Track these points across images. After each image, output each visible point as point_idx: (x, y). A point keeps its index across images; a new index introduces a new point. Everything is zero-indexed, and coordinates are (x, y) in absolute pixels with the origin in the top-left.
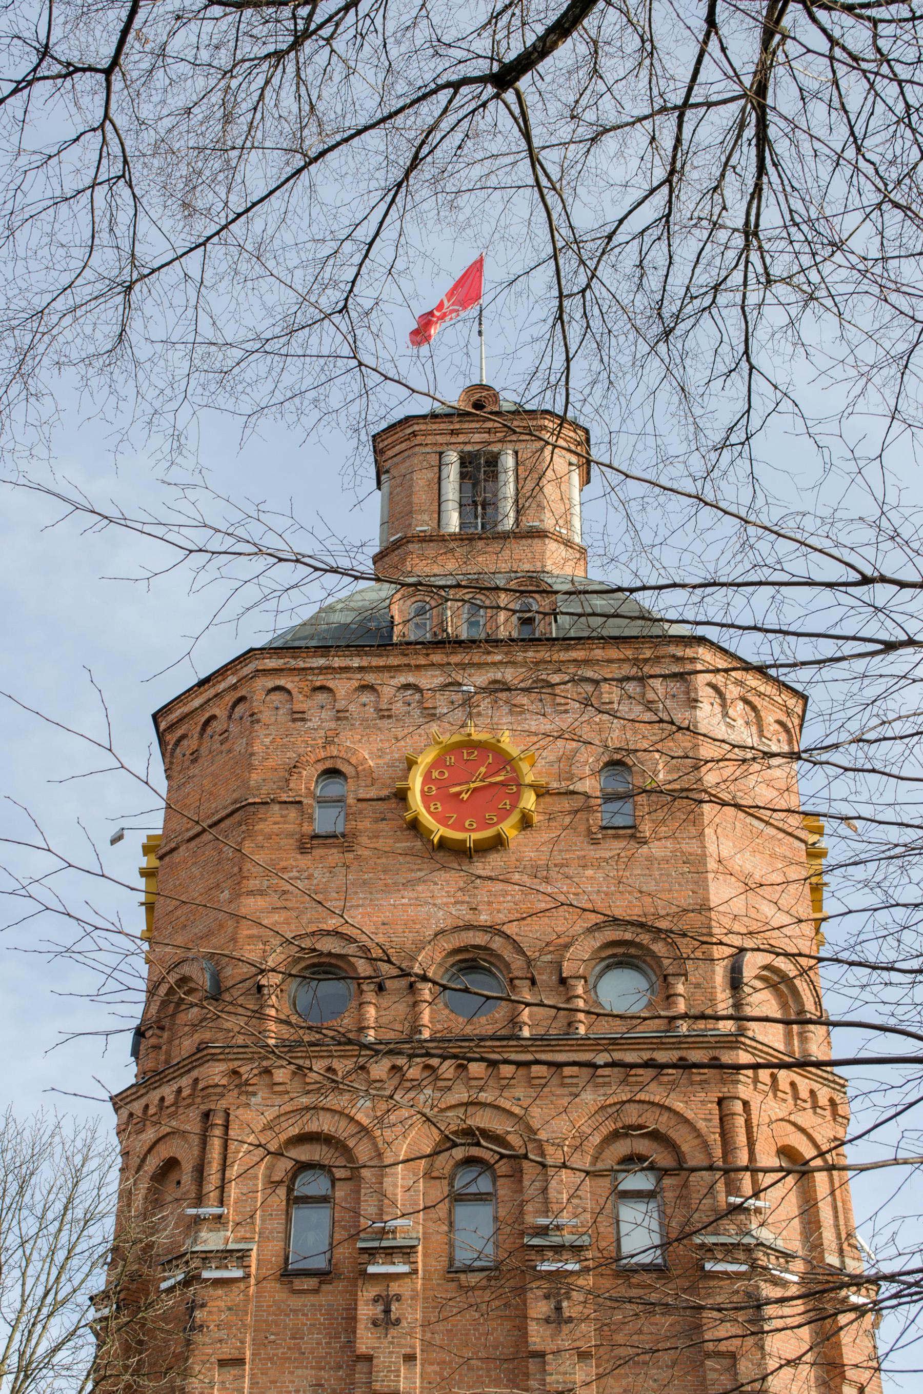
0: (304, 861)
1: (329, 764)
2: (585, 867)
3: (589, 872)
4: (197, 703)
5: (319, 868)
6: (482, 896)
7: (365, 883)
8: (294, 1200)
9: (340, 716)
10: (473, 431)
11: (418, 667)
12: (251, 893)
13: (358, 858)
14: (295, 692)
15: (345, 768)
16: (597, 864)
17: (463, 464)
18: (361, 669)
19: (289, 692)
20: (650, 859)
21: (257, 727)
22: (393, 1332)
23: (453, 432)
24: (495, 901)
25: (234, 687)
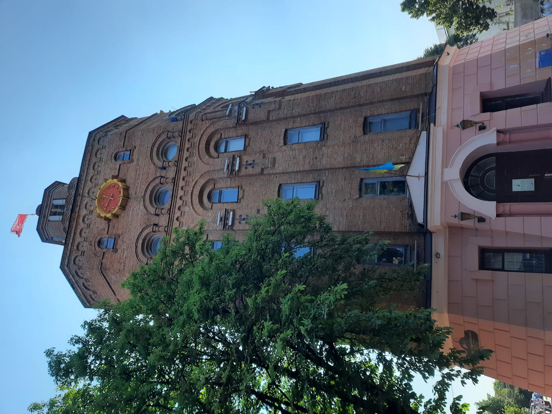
0: (119, 251)
1: (96, 244)
9: (85, 240)
10: (45, 211)
13: (122, 234)
15: (98, 238)
16: (138, 160)
18: (75, 234)
19: (76, 257)
24: (139, 188)
25: (73, 276)
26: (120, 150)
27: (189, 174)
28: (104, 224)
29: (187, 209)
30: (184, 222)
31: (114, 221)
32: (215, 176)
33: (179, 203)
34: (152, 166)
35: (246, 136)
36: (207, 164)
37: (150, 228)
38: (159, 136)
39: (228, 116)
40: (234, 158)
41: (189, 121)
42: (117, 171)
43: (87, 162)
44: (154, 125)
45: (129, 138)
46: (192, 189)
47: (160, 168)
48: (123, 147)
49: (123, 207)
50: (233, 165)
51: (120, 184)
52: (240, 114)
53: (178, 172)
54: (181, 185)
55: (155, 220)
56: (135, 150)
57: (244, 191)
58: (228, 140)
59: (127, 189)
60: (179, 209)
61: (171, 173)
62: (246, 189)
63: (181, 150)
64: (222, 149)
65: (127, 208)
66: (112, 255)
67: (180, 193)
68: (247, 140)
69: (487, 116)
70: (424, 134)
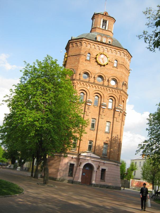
0: (86, 62)
1: (89, 52)
2: (112, 70)
3: (112, 70)
4: (75, 41)
6: (102, 70)
9: (91, 47)
12: (80, 64)
16: (113, 70)
18: (94, 43)
19: (86, 43)
20: (118, 71)
22: (89, 110)
23: (103, 17)
25: (80, 41)
26: (118, 62)
29: (94, 89)
31: (95, 60)
34: (110, 76)
35: (112, 109)
42: (111, 61)
43: (117, 48)
45: (121, 66)
56: (116, 69)
60: (95, 86)
62: (97, 108)
64: (111, 101)
69: (101, 169)
70: (99, 157)
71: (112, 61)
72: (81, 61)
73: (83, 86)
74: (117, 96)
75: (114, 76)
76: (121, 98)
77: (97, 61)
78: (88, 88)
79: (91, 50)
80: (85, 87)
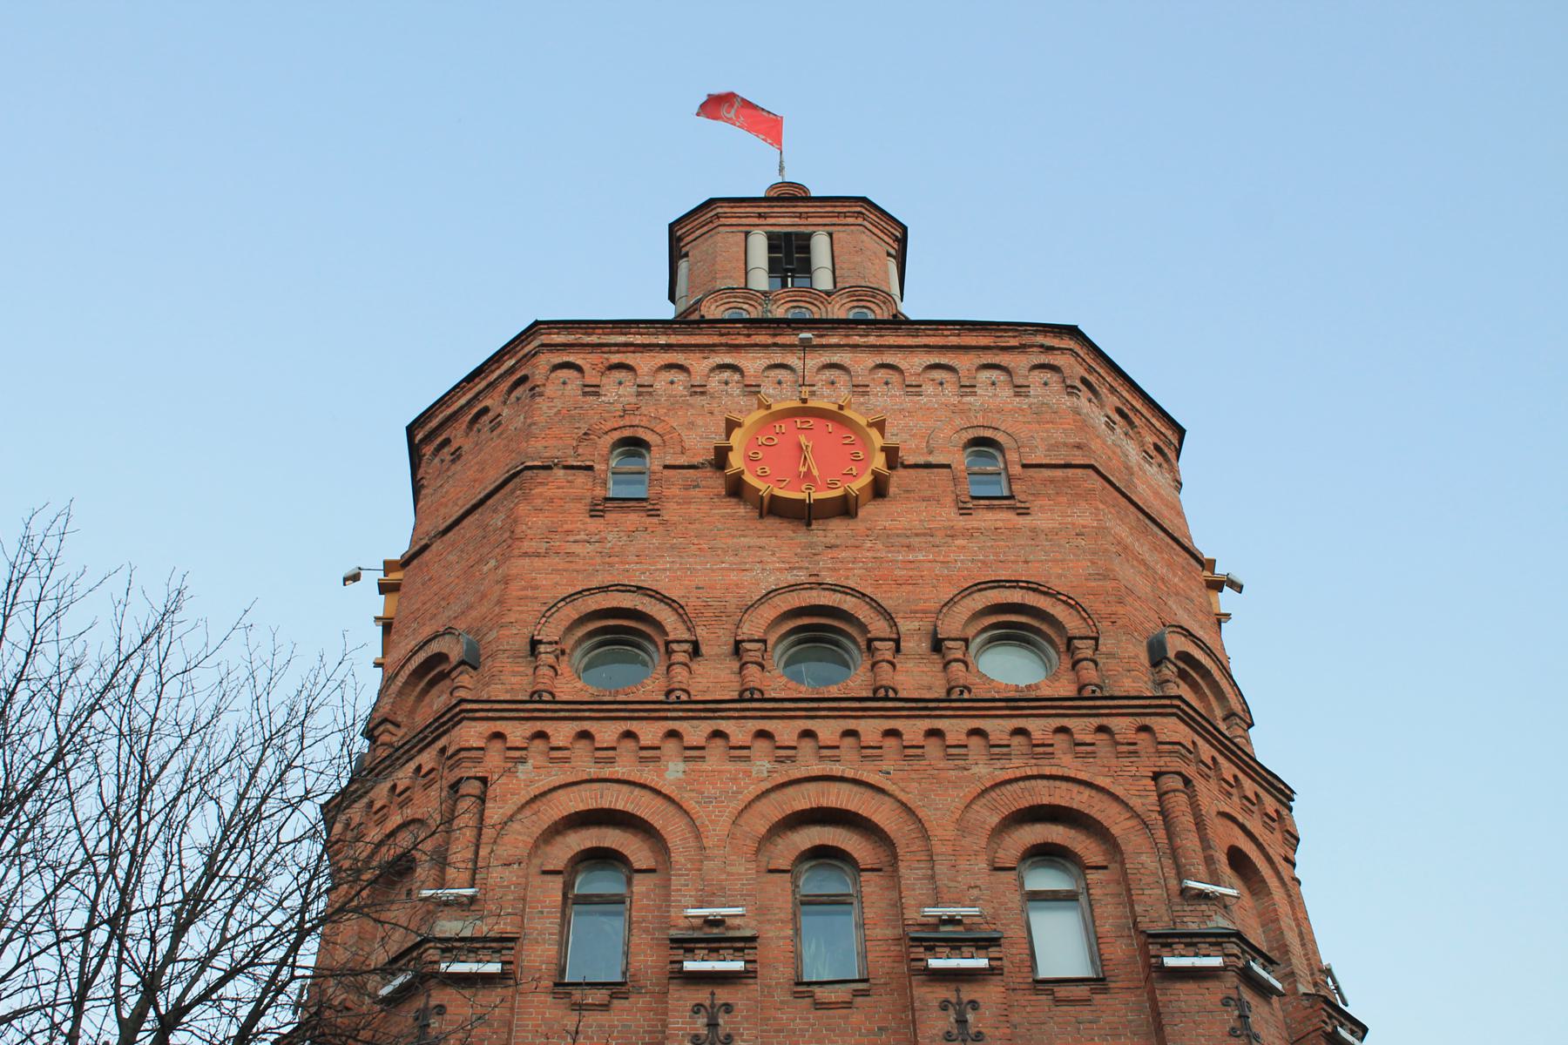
0: (595, 525)
1: (627, 433)
3: (959, 542)
5: (616, 529)
7: (673, 547)
8: (570, 900)
9: (644, 390)
11: (737, 348)
13: (664, 523)
14: (586, 368)
16: (969, 534)
17: (772, 248)
18: (668, 347)
19: (579, 369)
20: (1033, 530)
21: (538, 399)
23: (760, 216)
26: (1013, 456)
27: (911, 753)
28: (700, 446)
29: (762, 765)
30: (704, 766)
31: (716, 483)
32: (912, 873)
33: (786, 731)
34: (947, 593)
35: (1098, 983)
36: (962, 827)
37: (681, 627)
38: (1075, 606)
39: (1184, 891)
40: (983, 944)
41: (1147, 721)
42: (921, 460)
43: (954, 341)
44: (1127, 573)
45: (1066, 479)
46: (850, 774)
47: (935, 633)
48: (1025, 466)
49: (776, 509)
50: (955, 945)
51: (866, 479)
52: (1192, 941)
53: (919, 707)
54: (861, 725)
55: (715, 641)
56: (1011, 516)
57: (848, 1005)
58: (1083, 899)
59: (845, 508)
60: (762, 734)
61: (915, 676)
62: (856, 1017)
63: (1018, 704)
64: (1044, 880)
65: (772, 523)
66: (579, 499)
67: (829, 730)
68: (1081, 991)
71: (932, 459)
72: (534, 522)
73: (594, 771)
74: (1118, 790)
75: (998, 584)
76: (1179, 802)
77: (737, 489)
78: (673, 772)
79: (648, 409)
80: (619, 771)
